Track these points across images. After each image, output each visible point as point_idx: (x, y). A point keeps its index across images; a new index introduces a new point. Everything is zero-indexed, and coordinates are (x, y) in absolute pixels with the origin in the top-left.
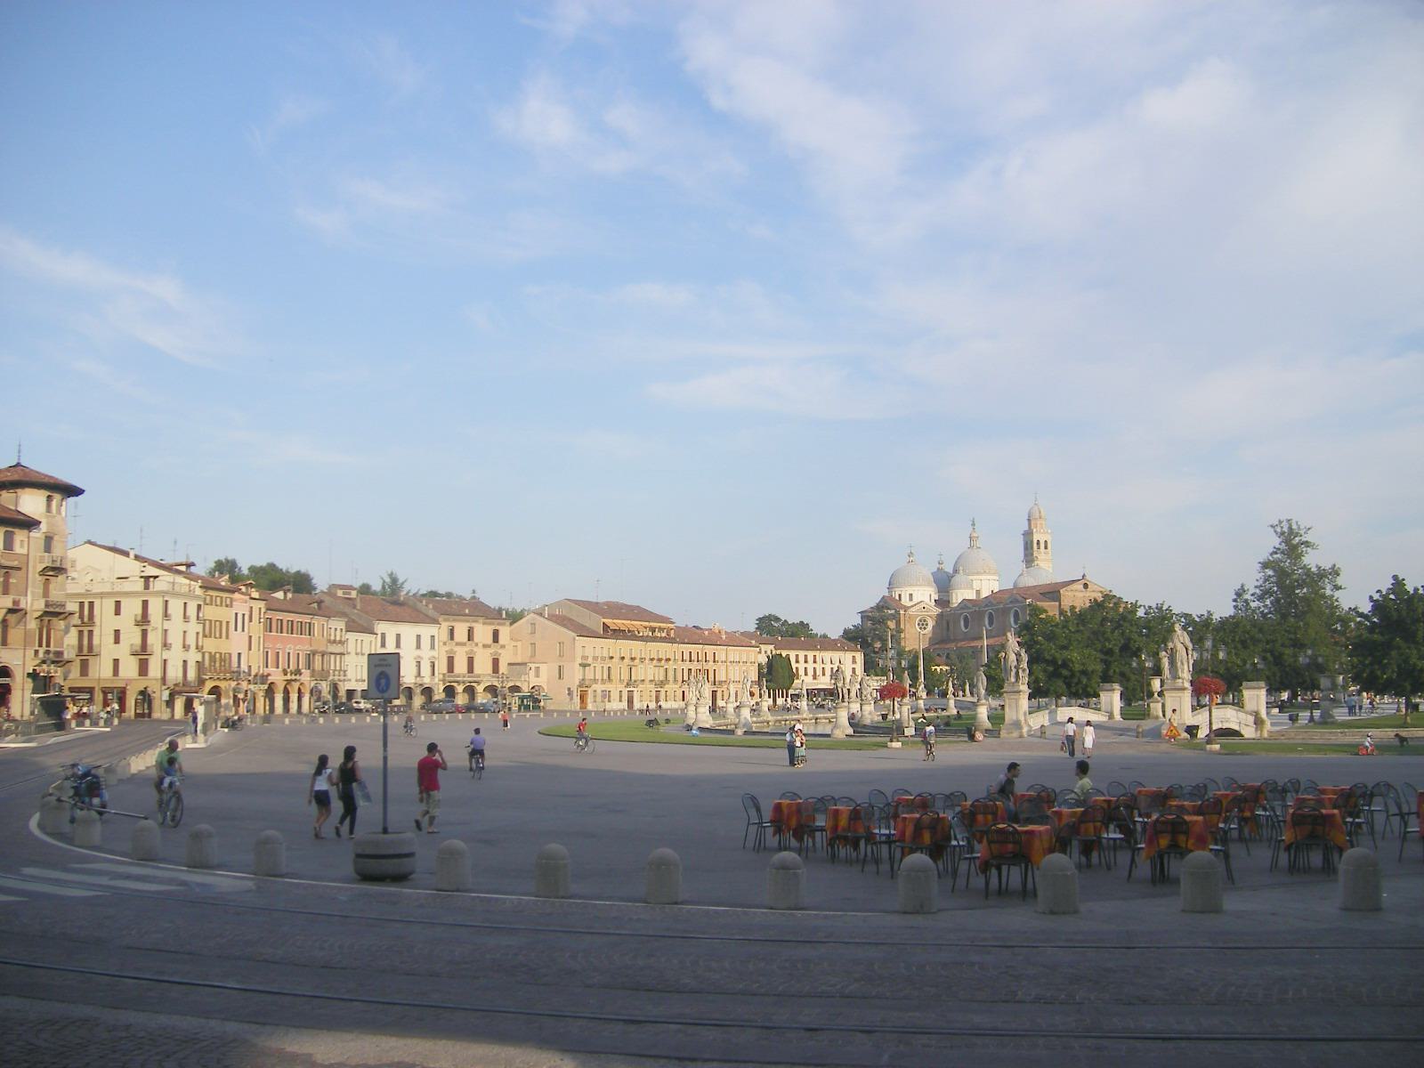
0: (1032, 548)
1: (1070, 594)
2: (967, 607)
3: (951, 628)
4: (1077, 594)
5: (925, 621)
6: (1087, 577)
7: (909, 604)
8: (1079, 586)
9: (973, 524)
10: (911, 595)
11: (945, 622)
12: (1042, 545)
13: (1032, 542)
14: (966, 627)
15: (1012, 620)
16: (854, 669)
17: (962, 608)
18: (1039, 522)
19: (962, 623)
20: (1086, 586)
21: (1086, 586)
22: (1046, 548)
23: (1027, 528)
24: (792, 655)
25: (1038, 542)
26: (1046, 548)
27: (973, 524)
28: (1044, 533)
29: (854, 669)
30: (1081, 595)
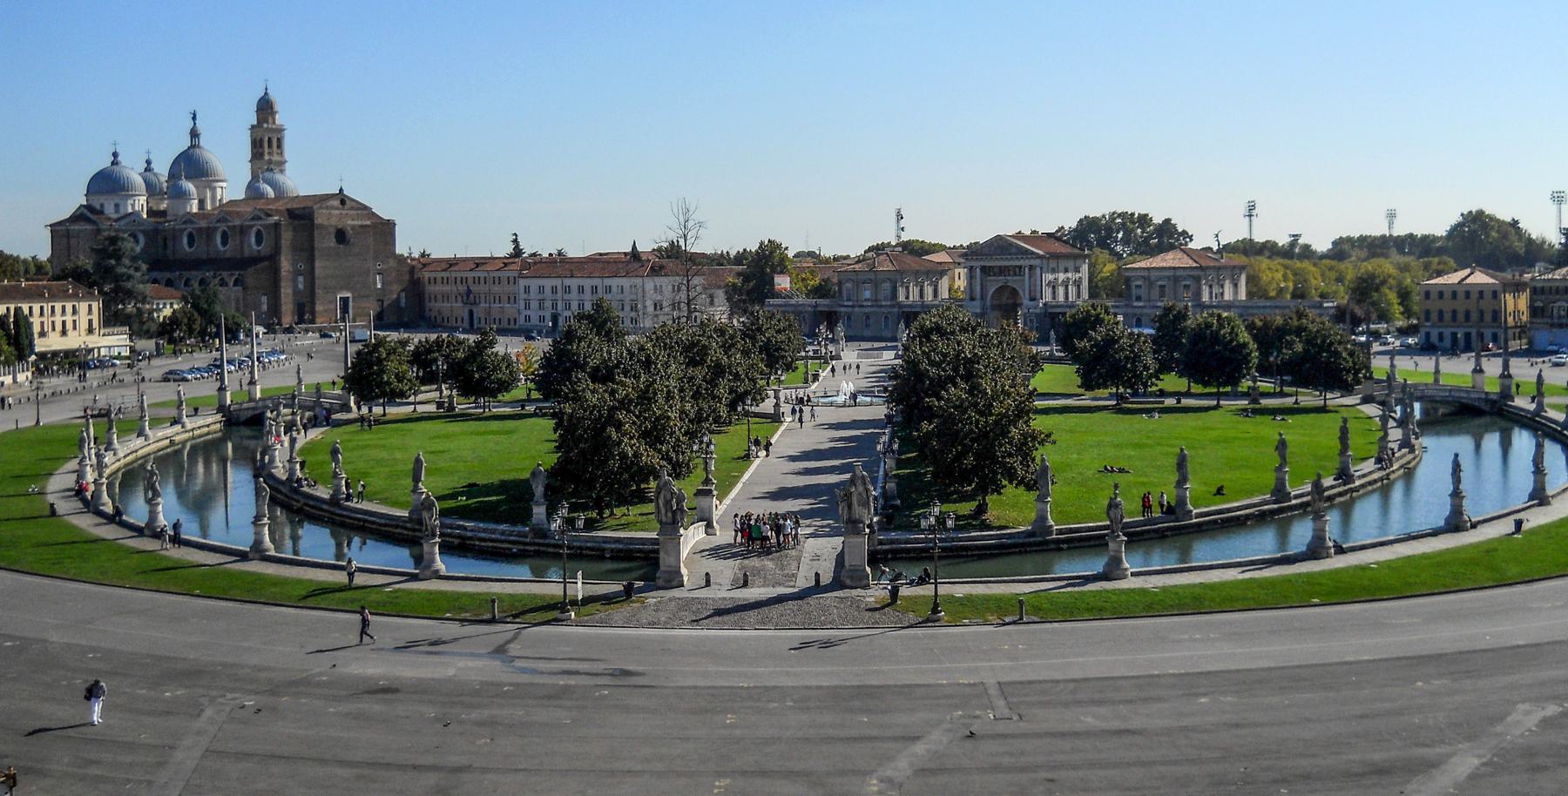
0: (261, 146)
7: (115, 216)
8: (336, 203)
9: (194, 118)
10: (117, 206)
13: (261, 141)
14: (191, 244)
15: (253, 240)
16: (90, 321)
19: (185, 240)
20: (343, 202)
24: (25, 308)
26: (279, 146)
27: (194, 118)
29: (90, 321)
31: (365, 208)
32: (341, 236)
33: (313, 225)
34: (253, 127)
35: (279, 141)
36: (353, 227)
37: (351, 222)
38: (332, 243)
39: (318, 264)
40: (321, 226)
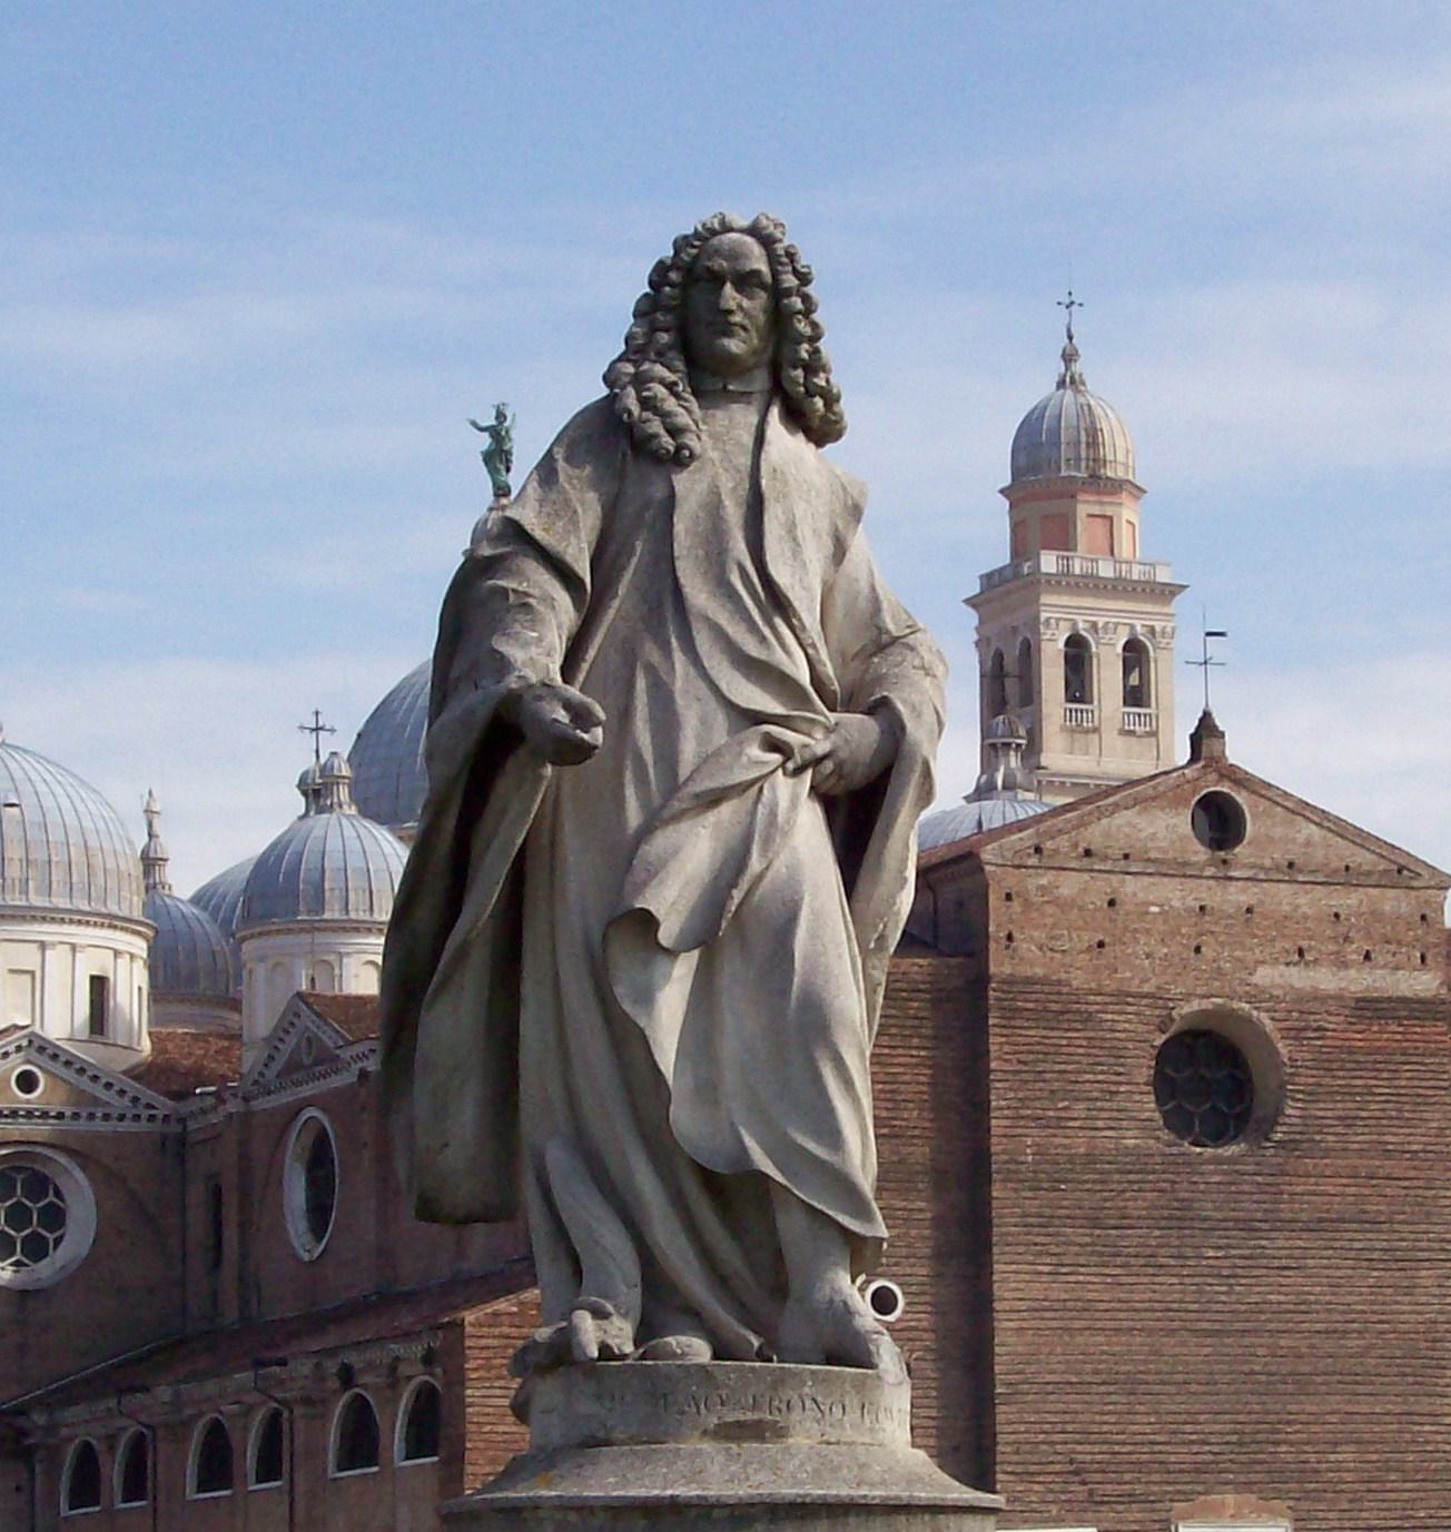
0: (1030, 694)
1: (1069, 885)
2: (327, 1061)
3: (231, 1235)
4: (1131, 887)
5: (39, 1184)
6: (1238, 751)
8: (1173, 828)
11: (197, 1194)
12: (1108, 677)
13: (1029, 653)
14: (319, 1213)
17: (293, 1070)
18: (1082, 510)
19: (296, 1191)
20: (1220, 821)
21: (1220, 821)
22: (1136, 696)
23: (1003, 558)
25: (1077, 655)
26: (1136, 696)
28: (1121, 588)
30: (1175, 895)
31: (1402, 871)
32: (1212, 1078)
33: (981, 980)
34: (989, 580)
35: (1135, 654)
36: (1303, 1012)
37: (1270, 983)
38: (1133, 1120)
39: (1015, 1282)
40: (1058, 1007)
